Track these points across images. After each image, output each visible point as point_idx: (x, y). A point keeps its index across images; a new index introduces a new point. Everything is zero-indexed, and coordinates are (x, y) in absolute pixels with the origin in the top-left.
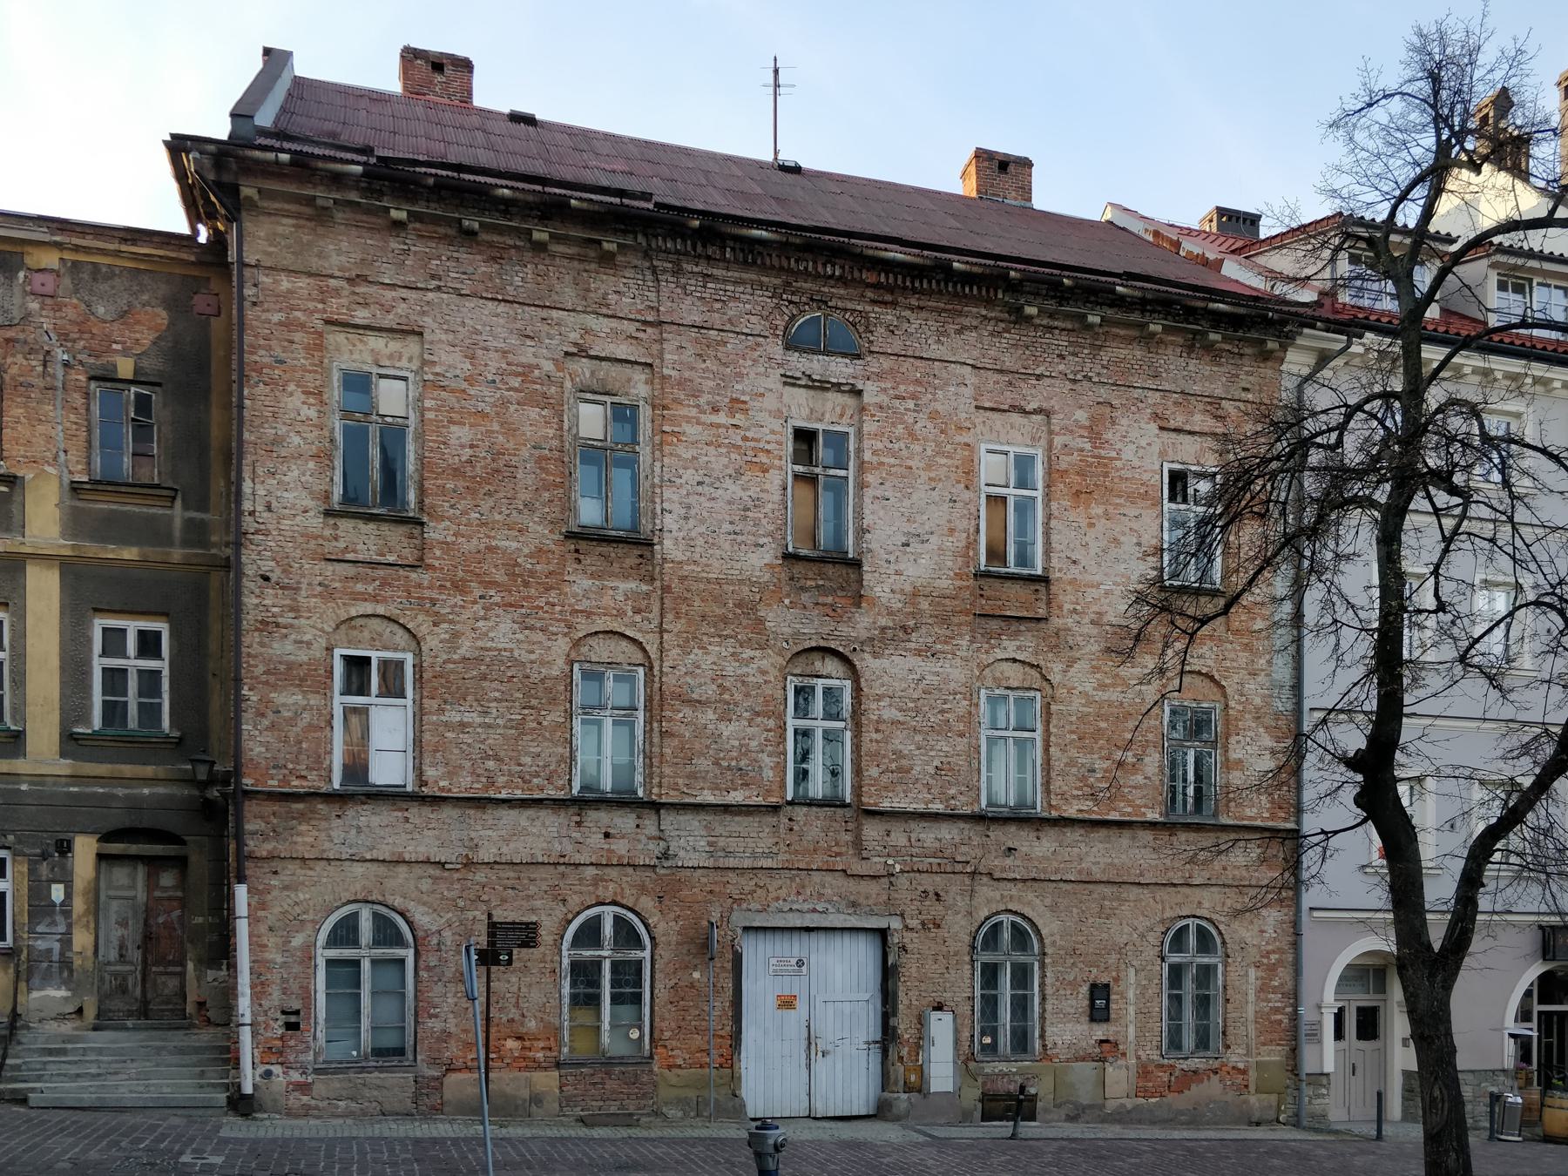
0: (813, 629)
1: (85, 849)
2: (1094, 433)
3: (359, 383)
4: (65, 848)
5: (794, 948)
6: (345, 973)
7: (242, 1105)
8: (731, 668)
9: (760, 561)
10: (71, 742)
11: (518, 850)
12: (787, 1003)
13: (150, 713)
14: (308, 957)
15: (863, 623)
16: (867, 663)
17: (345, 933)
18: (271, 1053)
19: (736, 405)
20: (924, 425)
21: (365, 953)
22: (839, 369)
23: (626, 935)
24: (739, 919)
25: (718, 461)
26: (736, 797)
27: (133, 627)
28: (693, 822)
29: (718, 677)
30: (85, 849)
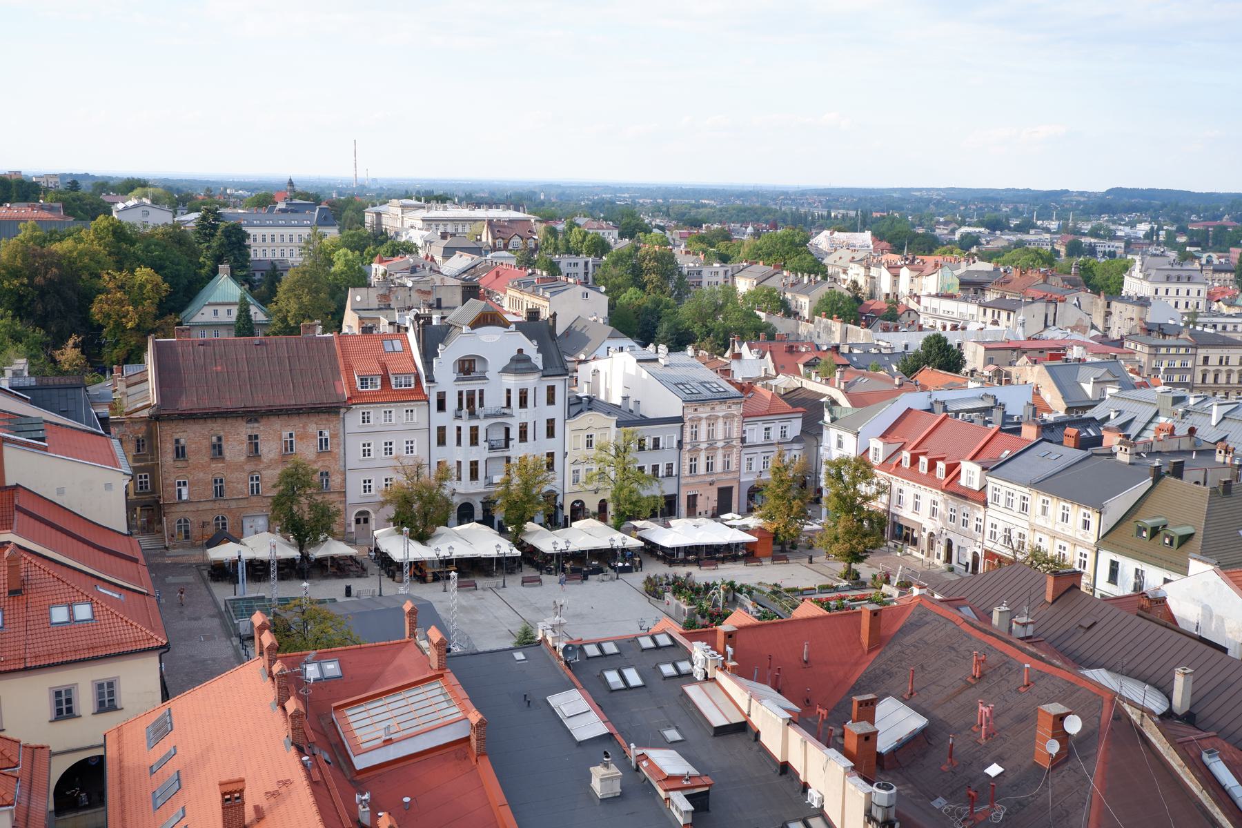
1: (139, 509)
2: (304, 427)
4: (136, 509)
5: (252, 518)
6: (180, 527)
7: (166, 548)
8: (239, 476)
9: (243, 458)
10: (136, 494)
11: (204, 508)
12: (251, 527)
13: (146, 487)
14: (174, 526)
15: (262, 466)
16: (263, 472)
17: (180, 522)
18: (170, 540)
19: (238, 434)
20: (271, 432)
21: (183, 524)
23: (223, 518)
24: (242, 515)
25: (235, 443)
26: (241, 497)
27: (143, 475)
28: (234, 501)
29: (237, 478)
30: (139, 509)
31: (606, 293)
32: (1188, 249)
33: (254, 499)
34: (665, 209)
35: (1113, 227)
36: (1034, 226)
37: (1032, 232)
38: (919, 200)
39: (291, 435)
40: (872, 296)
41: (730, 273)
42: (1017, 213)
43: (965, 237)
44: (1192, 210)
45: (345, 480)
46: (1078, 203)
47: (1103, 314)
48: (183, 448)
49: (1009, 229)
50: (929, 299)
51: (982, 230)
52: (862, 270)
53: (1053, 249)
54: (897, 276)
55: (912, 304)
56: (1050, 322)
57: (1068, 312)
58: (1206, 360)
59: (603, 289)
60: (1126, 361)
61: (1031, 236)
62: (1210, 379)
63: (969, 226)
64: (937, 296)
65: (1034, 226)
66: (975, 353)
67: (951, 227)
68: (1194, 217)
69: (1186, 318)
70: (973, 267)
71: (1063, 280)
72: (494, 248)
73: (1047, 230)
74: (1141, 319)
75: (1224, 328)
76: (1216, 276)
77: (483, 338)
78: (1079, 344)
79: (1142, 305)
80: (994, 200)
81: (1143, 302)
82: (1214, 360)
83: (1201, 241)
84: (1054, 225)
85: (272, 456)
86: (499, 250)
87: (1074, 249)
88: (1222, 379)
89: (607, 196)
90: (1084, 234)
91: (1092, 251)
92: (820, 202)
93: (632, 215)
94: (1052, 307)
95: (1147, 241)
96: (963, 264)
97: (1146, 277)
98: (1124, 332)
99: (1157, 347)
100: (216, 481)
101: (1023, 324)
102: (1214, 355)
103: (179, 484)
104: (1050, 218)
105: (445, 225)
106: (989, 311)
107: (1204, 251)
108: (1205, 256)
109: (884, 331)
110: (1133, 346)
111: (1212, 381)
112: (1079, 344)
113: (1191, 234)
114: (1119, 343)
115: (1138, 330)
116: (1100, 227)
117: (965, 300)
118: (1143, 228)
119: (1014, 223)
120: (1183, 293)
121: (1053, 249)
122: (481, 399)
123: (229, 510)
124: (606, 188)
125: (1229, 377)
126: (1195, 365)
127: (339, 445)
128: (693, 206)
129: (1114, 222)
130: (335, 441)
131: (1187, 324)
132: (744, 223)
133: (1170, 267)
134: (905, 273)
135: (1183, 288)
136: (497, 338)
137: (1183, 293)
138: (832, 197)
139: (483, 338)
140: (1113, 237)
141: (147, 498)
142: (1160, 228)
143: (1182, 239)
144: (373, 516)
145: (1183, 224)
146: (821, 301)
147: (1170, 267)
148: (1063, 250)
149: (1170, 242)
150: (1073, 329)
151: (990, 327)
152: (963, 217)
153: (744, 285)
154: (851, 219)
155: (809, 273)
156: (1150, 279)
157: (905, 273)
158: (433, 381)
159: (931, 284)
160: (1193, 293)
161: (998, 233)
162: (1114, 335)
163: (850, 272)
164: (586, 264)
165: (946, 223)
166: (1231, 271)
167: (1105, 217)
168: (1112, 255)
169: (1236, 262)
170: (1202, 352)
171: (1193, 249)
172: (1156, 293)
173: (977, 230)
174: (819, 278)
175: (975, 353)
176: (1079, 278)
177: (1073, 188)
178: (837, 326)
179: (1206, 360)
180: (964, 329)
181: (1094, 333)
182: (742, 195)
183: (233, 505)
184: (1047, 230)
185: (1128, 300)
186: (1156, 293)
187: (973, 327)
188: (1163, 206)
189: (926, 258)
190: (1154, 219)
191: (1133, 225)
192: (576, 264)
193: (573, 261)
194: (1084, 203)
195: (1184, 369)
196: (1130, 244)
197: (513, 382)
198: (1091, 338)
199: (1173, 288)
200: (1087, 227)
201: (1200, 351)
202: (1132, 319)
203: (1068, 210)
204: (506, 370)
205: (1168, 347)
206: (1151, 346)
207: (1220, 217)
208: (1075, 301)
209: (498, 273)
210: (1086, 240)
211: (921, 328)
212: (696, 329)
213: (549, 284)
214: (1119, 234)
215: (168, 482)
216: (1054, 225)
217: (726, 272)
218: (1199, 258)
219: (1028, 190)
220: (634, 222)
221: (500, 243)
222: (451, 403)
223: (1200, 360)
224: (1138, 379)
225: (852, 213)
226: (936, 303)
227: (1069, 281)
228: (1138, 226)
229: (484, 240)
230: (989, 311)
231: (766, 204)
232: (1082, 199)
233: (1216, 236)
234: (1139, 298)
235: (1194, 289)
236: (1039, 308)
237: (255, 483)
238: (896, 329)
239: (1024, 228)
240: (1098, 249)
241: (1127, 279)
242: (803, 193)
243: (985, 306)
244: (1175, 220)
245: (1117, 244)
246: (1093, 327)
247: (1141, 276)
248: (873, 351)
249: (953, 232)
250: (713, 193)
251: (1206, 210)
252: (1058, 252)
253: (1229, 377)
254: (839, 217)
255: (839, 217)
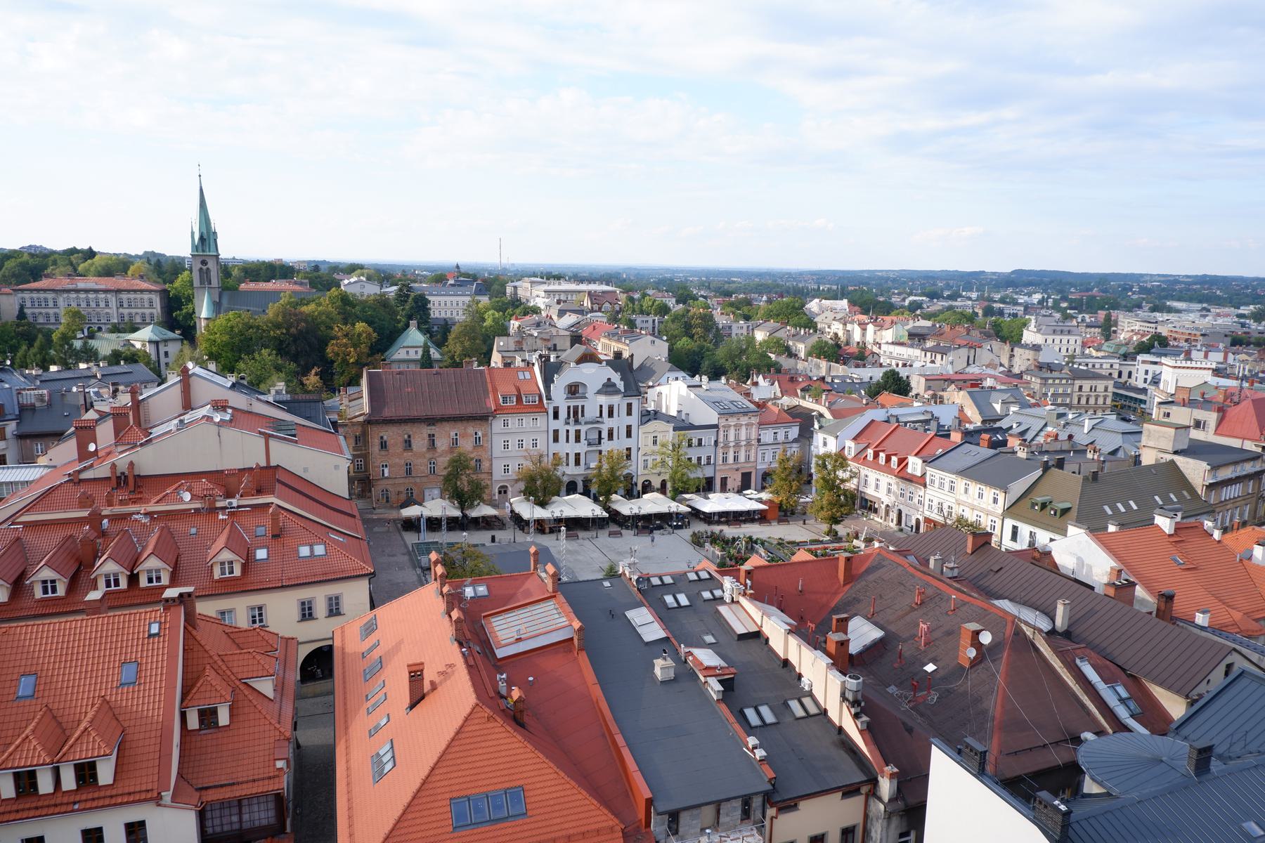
0: (431, 456)
1: (356, 482)
2: (465, 429)
3: (382, 438)
7: (374, 508)
9: (425, 450)
10: (354, 472)
15: (437, 455)
17: (383, 491)
22: (433, 427)
23: (411, 489)
30: (356, 482)
31: (667, 341)
32: (1068, 311)
33: (431, 477)
34: (707, 284)
35: (1016, 297)
36: (961, 296)
37: (959, 300)
38: (881, 278)
39: (456, 435)
40: (848, 343)
41: (751, 328)
42: (948, 287)
43: (911, 303)
44: (1072, 285)
45: (491, 465)
46: (992, 280)
47: (1008, 356)
48: (385, 442)
49: (943, 297)
50: (887, 345)
51: (924, 298)
52: (841, 326)
53: (974, 311)
54: (864, 330)
55: (875, 349)
56: (971, 362)
57: (984, 355)
58: (1081, 388)
59: (665, 338)
60: (1024, 388)
61: (959, 303)
62: (1083, 401)
63: (915, 296)
64: (893, 343)
65: (961, 296)
66: (918, 382)
67: (902, 297)
68: (1072, 290)
69: (1066, 359)
70: (917, 324)
71: (981, 333)
72: (592, 311)
73: (970, 299)
74: (1035, 360)
75: (1094, 366)
76: (1088, 330)
77: (584, 371)
78: (991, 376)
79: (1036, 350)
80: (932, 278)
81: (1037, 348)
82: (1086, 388)
83: (1078, 306)
84: (974, 295)
85: (443, 448)
86: (596, 311)
87: (989, 312)
88: (1092, 401)
89: (668, 276)
90: (995, 301)
91: (1001, 312)
92: (813, 279)
93: (685, 288)
94: (973, 351)
95: (1040, 306)
96: (911, 322)
97: (1039, 331)
98: (1023, 368)
99: (1046, 379)
100: (407, 464)
101: (952, 363)
102: (1087, 385)
103: (383, 466)
104: (971, 290)
105: (559, 295)
106: (929, 354)
107: (1080, 312)
108: (1080, 316)
109: (856, 367)
110: (1029, 378)
111: (1085, 403)
112: (991, 376)
113: (1071, 301)
114: (1020, 376)
115: (1033, 367)
116: (1007, 296)
117: (912, 346)
118: (1037, 297)
119: (946, 293)
120: (1065, 342)
121: (974, 311)
122: (583, 411)
123: (415, 484)
124: (668, 270)
125: (1096, 400)
126: (1072, 392)
127: (487, 441)
128: (726, 282)
129: (1017, 293)
130: (485, 439)
131: (1067, 363)
132: (761, 294)
133: (1055, 324)
134: (870, 328)
135: (1065, 339)
136: (594, 370)
137: (1065, 342)
138: (821, 277)
139: (584, 371)
140: (1016, 303)
141: (361, 475)
142: (1049, 297)
143: (1064, 305)
144: (510, 489)
145: (1065, 294)
146: (813, 347)
147: (1055, 324)
148: (980, 312)
149: (1056, 307)
150: (987, 366)
151: (929, 365)
152: (911, 290)
153: (760, 336)
154: (834, 291)
155: (805, 328)
156: (1042, 332)
157: (870, 328)
158: (551, 399)
159: (888, 335)
160: (1072, 342)
161: (935, 300)
162: (1016, 370)
163: (833, 327)
164: (654, 321)
165: (899, 294)
166: (1099, 327)
167: (1010, 290)
168: (1015, 315)
169: (1102, 320)
170: (1078, 383)
171: (1072, 312)
172: (1046, 342)
173: (921, 298)
174: (811, 331)
175: (918, 382)
176: (992, 331)
177: (989, 268)
178: (824, 364)
179: (1081, 388)
180: (911, 366)
181: (1002, 369)
182: (760, 275)
183: (418, 480)
184: (970, 299)
185: (1026, 346)
186: (1046, 342)
187: (917, 365)
188: (1051, 282)
189: (885, 318)
190: (1045, 291)
191: (1029, 295)
192: (647, 321)
193: (645, 319)
194: (996, 280)
195: (1065, 395)
196: (1028, 308)
197: (604, 400)
198: (1000, 373)
199: (1057, 338)
200: (997, 296)
201: (1076, 382)
202: (1029, 360)
203: (985, 285)
204: (599, 392)
205: (1054, 379)
206: (1042, 378)
207: (1091, 290)
208: (989, 347)
209: (594, 327)
210: (996, 305)
211: (881, 365)
212: (728, 365)
213: (629, 335)
214: (1020, 301)
215: (376, 464)
216: (974, 295)
217: (748, 327)
218: (1076, 318)
219: (957, 271)
220: (686, 293)
221: (596, 307)
222: (563, 414)
223: (1076, 388)
224: (1033, 401)
225: (835, 287)
226: (892, 348)
227: (985, 334)
228: (1033, 296)
229: (585, 305)
230: (929, 354)
231: (776, 281)
232: (994, 277)
233: (1087, 303)
234: (1034, 345)
235: (1072, 339)
236: (964, 352)
237: (432, 466)
238: (864, 366)
239: (953, 297)
240: (1005, 311)
241: (1025, 332)
242: (801, 274)
243: (926, 350)
244: (1060, 292)
245: (1018, 308)
246: (1001, 365)
247: (1035, 330)
248: (848, 381)
249: (904, 300)
250: (740, 274)
251: (1081, 285)
252: (977, 313)
253: (1096, 400)
254: (826, 289)
255: (826, 289)
